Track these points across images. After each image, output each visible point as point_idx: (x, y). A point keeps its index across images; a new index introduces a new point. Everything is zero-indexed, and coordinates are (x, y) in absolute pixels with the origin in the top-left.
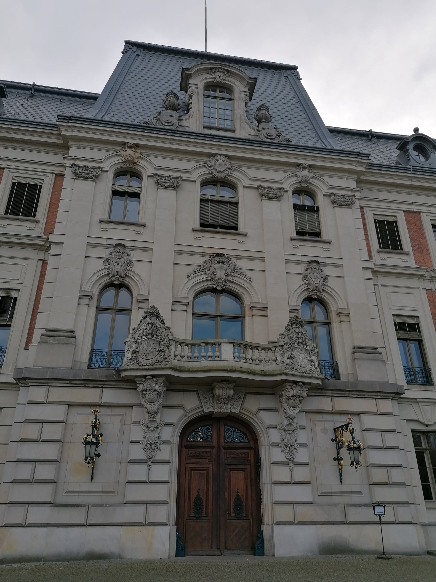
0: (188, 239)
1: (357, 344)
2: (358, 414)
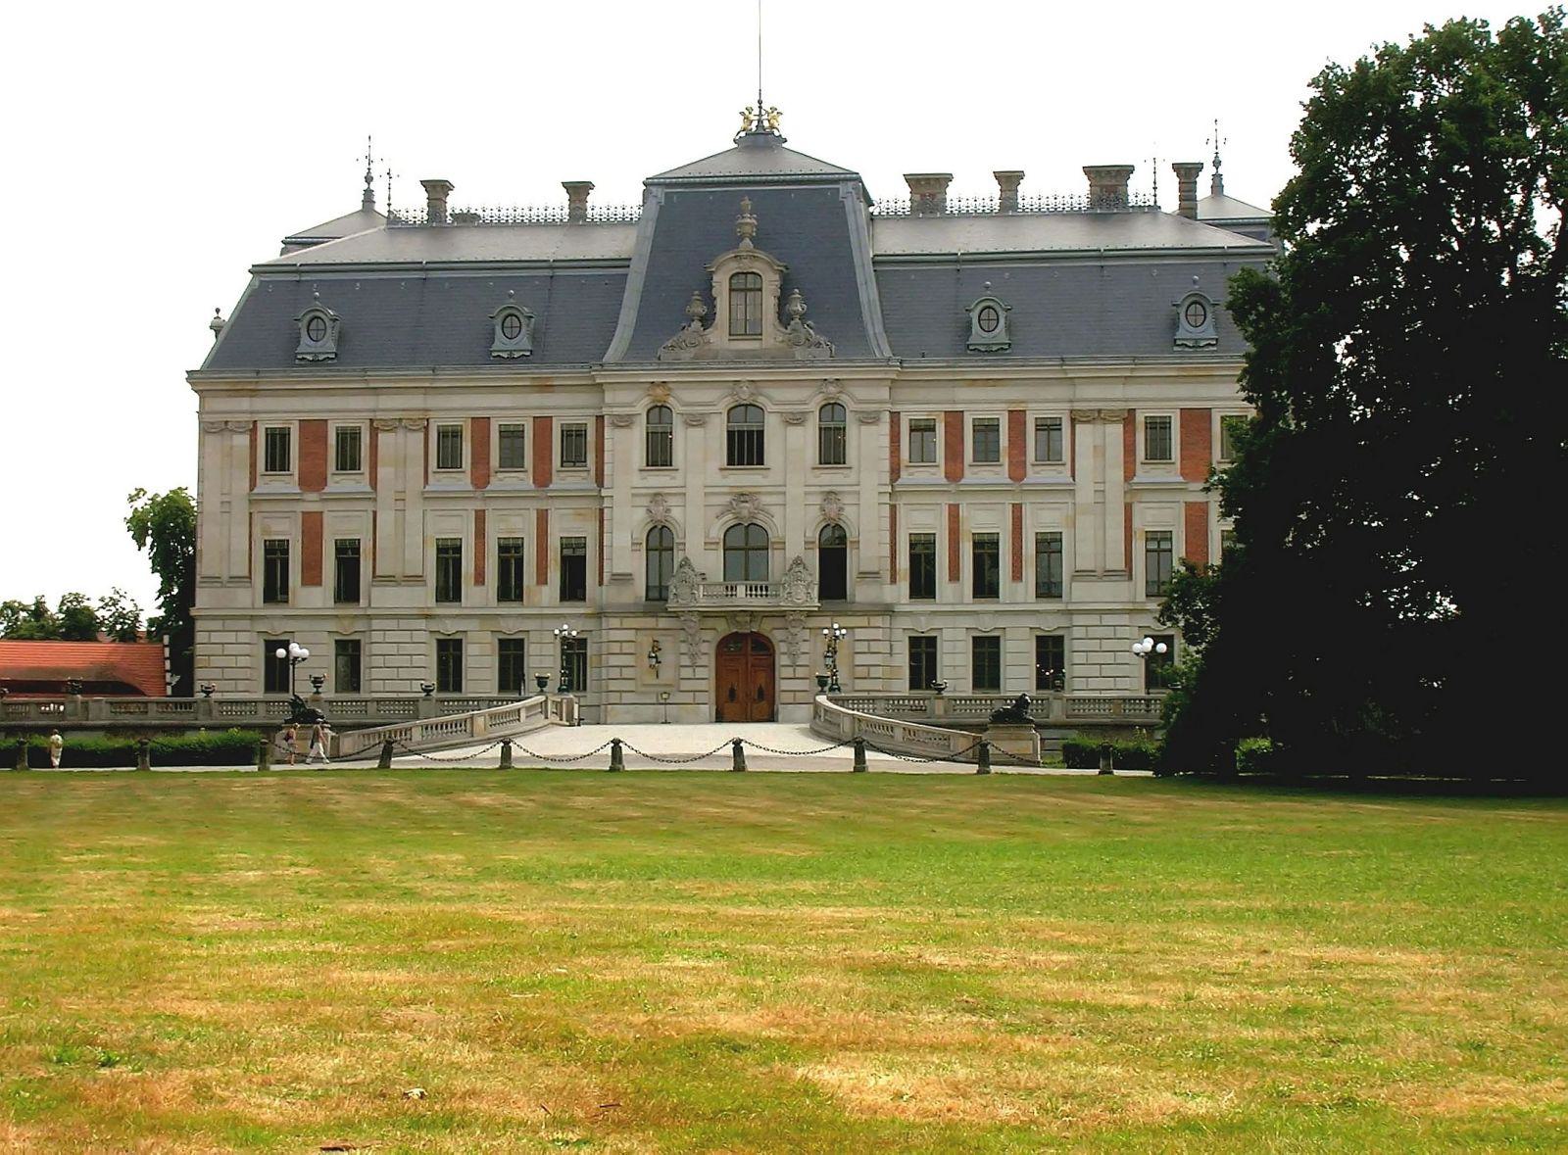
0: (717, 478)
1: (862, 569)
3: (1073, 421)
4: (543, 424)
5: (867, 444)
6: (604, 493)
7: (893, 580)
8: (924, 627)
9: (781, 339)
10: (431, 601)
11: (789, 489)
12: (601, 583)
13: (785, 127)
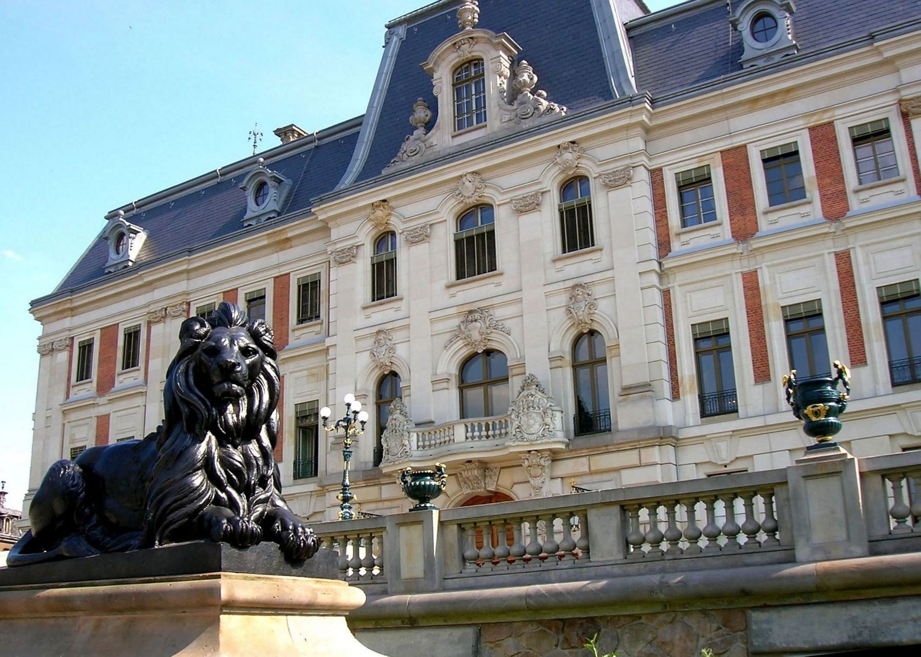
2: (618, 470)
3: (905, 117)
4: (281, 282)
5: (622, 215)
6: (329, 342)
7: (676, 395)
9: (507, 118)
11: (526, 295)
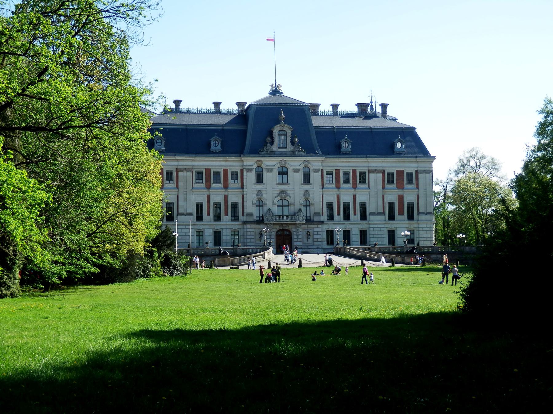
3: (369, 173)
4: (226, 171)
8: (331, 227)
10: (195, 220)
12: (243, 215)
13: (283, 89)
